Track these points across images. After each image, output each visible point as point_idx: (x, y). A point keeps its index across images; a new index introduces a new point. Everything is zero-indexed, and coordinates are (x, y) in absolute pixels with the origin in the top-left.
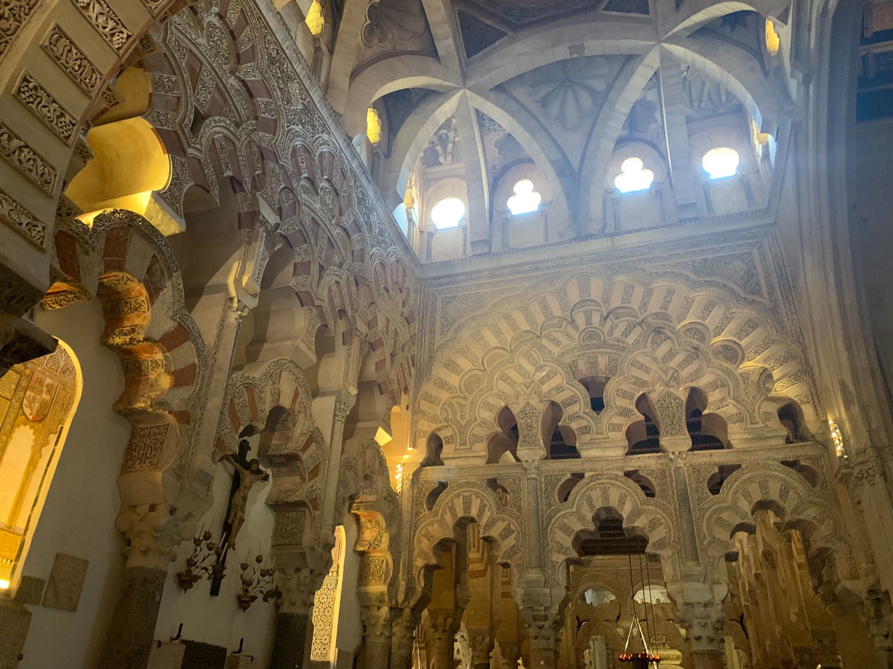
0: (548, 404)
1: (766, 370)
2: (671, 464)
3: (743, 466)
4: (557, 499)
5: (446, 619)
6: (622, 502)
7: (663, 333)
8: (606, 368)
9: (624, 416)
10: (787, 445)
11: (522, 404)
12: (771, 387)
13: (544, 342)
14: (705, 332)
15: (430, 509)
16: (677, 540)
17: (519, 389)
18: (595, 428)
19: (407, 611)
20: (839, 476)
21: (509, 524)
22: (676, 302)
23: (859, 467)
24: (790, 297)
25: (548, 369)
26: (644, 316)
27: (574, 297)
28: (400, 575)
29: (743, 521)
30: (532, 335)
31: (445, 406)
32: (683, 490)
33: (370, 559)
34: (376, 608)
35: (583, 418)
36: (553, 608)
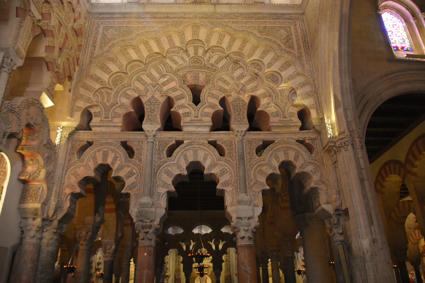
0: (166, 98)
1: (293, 89)
2: (236, 138)
3: (276, 142)
4: (165, 155)
5: (87, 233)
6: (205, 159)
7: (239, 64)
8: (204, 81)
9: (212, 108)
10: (300, 132)
11: (149, 96)
12: (295, 99)
13: (168, 61)
14: (262, 65)
15: (79, 158)
17: (148, 87)
18: (194, 114)
19: (55, 223)
20: (327, 147)
22: (248, 47)
23: (341, 141)
24: (309, 52)
25: (168, 77)
27: (189, 37)
28: (52, 198)
29: (273, 172)
30: (160, 56)
31: (97, 93)
33: (30, 186)
34: (32, 219)
35: (187, 108)
36: (156, 221)
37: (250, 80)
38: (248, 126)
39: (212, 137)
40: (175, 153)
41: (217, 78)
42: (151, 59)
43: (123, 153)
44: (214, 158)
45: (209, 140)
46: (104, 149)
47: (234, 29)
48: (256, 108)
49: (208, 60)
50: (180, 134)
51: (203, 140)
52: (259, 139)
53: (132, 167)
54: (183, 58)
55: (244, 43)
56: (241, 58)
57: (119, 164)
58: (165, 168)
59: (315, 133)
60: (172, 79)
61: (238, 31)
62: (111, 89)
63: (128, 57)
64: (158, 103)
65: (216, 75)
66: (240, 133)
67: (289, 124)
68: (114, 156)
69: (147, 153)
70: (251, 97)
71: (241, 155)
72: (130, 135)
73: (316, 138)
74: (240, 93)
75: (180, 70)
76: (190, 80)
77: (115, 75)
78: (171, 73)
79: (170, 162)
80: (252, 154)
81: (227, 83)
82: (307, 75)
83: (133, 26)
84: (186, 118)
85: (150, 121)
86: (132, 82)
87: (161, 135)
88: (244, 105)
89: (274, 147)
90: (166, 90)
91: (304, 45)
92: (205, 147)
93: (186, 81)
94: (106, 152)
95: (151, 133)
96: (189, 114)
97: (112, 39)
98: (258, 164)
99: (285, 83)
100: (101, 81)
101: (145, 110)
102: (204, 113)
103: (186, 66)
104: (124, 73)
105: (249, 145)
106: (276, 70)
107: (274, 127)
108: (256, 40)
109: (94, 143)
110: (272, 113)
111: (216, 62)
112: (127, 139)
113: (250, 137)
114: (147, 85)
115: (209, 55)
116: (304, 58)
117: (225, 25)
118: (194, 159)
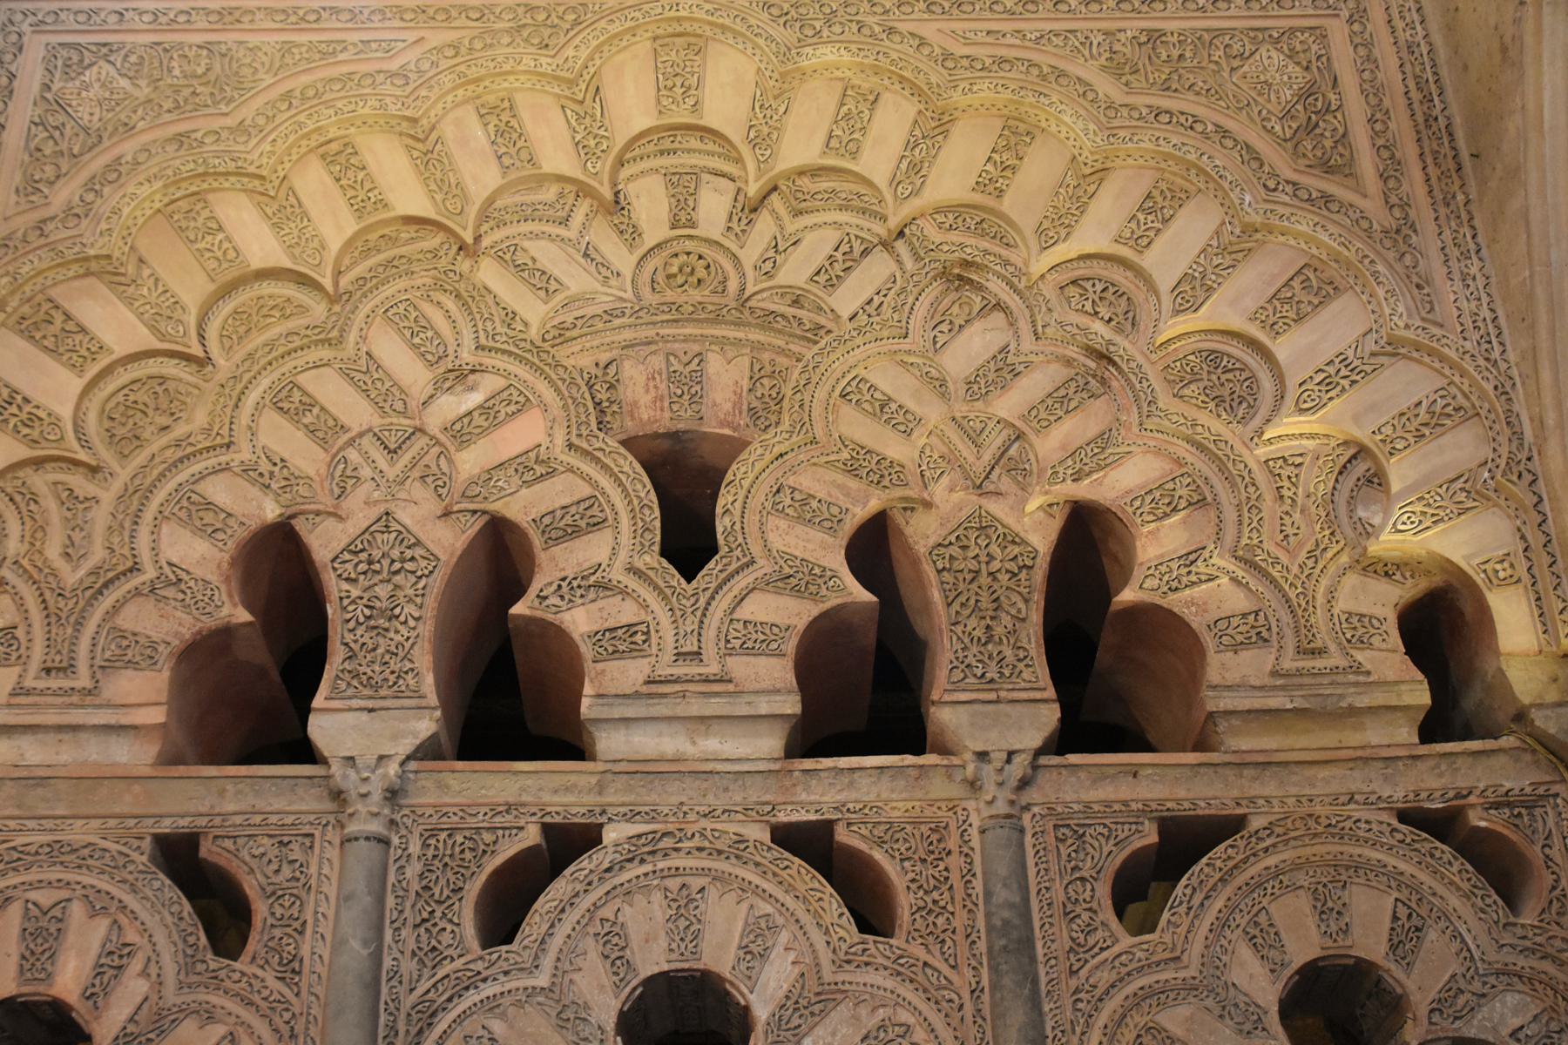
0: (475, 526)
1: (1361, 451)
2: (971, 805)
3: (1256, 823)
4: (469, 930)
6: (753, 953)
7: (979, 288)
8: (737, 405)
9: (797, 592)
10: (1424, 749)
11: (359, 516)
12: (1376, 521)
13: (489, 273)
14: (1139, 295)
17: (353, 455)
24: (1460, 197)
25: (489, 384)
26: (907, 210)
30: (434, 241)
32: (1012, 906)
35: (624, 592)
37: (1062, 392)
38: (1051, 715)
39: (804, 796)
40: (537, 918)
41: (828, 387)
42: (372, 262)
43: (169, 919)
45: (783, 817)
46: (33, 895)
47: (937, 51)
48: (1105, 593)
49: (769, 265)
50: (573, 778)
52: (1134, 806)
53: (233, 1019)
54: (591, 251)
55: (1007, 147)
56: (997, 250)
57: (139, 999)
58: (469, 1026)
59: (1528, 757)
60: (521, 399)
61: (965, 62)
62: (94, 470)
63: (219, 254)
64: (424, 563)
65: (822, 368)
66: (999, 765)
67: (1342, 697)
68: (108, 940)
69: (337, 912)
70: (1067, 510)
71: (1006, 923)
72: (222, 793)
73: (1541, 791)
74: (992, 488)
75: (575, 333)
76: (645, 399)
77: (123, 377)
78: (510, 353)
79: (502, 978)
80: (1085, 916)
81: (901, 419)
82: (1453, 355)
83: (253, 40)
84: (613, 666)
85: (367, 692)
86: (244, 418)
87: (443, 787)
88: (1020, 568)
89: (1245, 861)
90: (477, 471)
91: (1427, 150)
92: (751, 866)
93: (615, 407)
94: (46, 913)
95: (373, 772)
96: (639, 638)
97: (110, 129)
98: (1129, 989)
99: (1302, 411)
100: (24, 416)
101: (330, 611)
102: (740, 626)
103: (618, 305)
104: (188, 358)
105: (1064, 852)
106: (1237, 323)
107: (1235, 722)
108: (1092, 126)
110: (1222, 625)
111: (822, 278)
112: (203, 821)
113: (1069, 797)
114: (346, 437)
115: (774, 230)
116: (1428, 239)
117: (877, 29)
118: (674, 956)
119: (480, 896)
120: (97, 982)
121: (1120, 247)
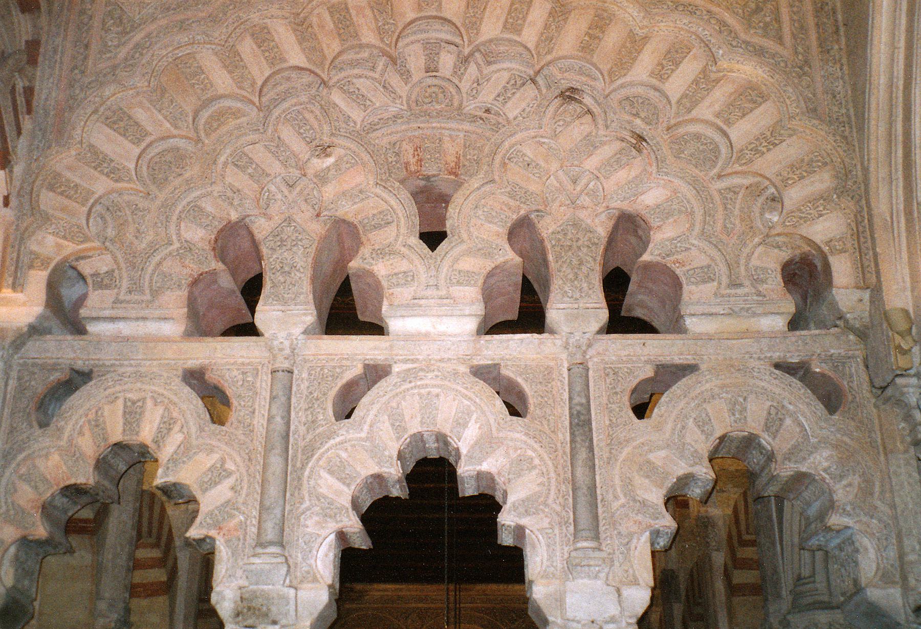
4: (330, 412)
6: (462, 424)
7: (581, 102)
11: (277, 219)
13: (337, 97)
16: (561, 500)
17: (273, 188)
21: (223, 461)
32: (582, 405)
37: (619, 156)
38: (604, 315)
44: (492, 421)
45: (475, 362)
46: (129, 395)
49: (475, 91)
51: (455, 361)
64: (307, 241)
80: (618, 409)
109: (94, 375)
111: (501, 99)
119: (337, 396)
120: (159, 435)
121: (651, 79)
